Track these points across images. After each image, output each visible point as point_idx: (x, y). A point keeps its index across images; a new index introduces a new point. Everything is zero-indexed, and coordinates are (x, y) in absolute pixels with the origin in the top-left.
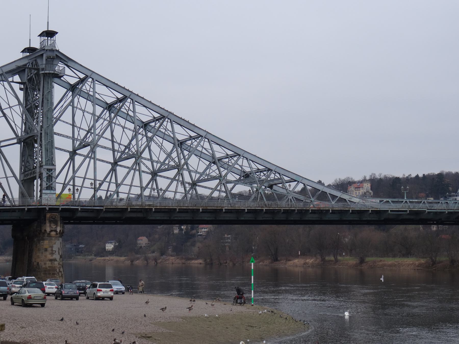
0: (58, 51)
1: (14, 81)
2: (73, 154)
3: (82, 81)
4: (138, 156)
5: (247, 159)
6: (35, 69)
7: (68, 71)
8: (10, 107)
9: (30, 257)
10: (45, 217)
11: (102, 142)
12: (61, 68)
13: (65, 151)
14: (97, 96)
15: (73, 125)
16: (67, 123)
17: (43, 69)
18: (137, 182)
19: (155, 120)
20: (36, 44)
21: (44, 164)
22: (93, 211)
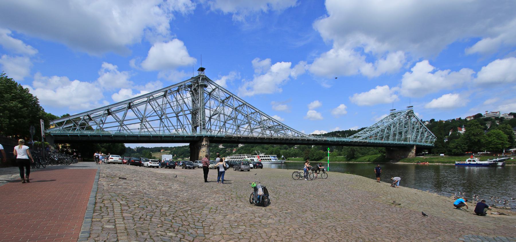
10: (203, 139)
19: (240, 106)
21: (202, 119)
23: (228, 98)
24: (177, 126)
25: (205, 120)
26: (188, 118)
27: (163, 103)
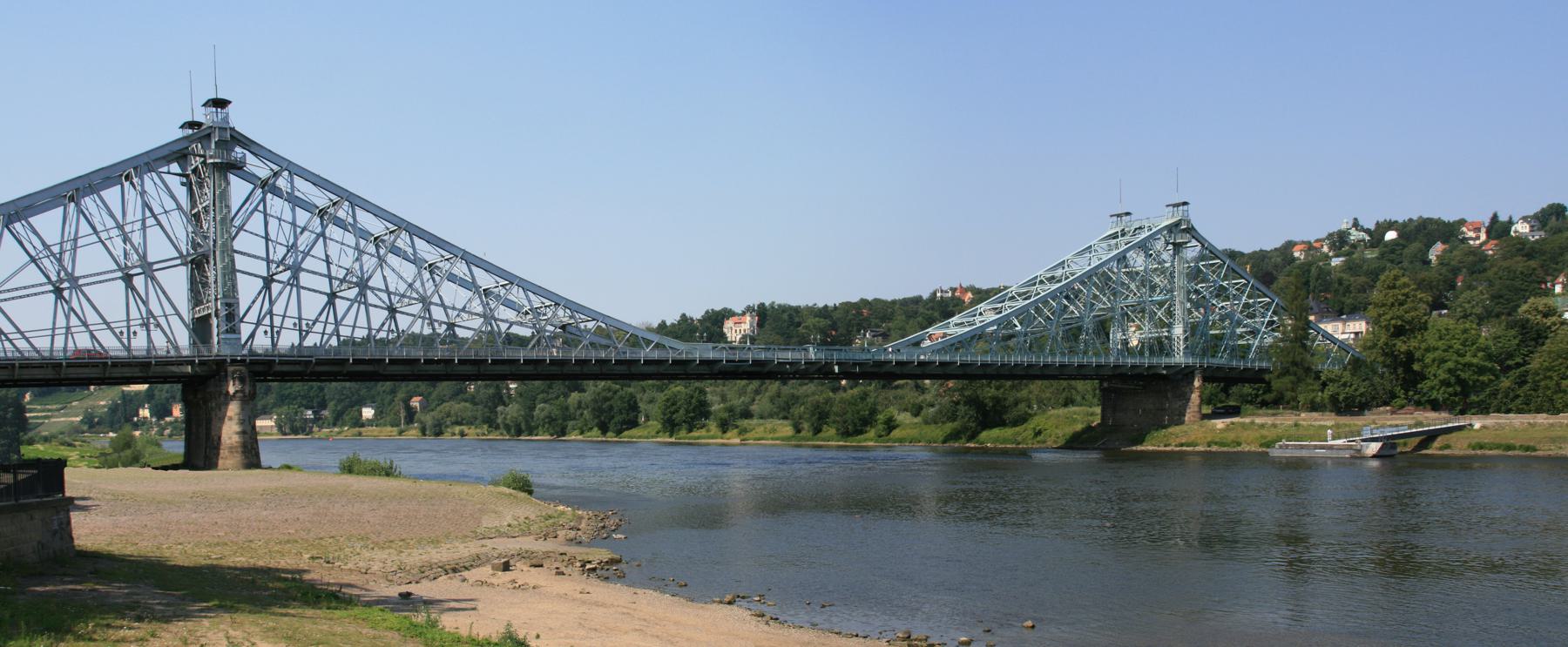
0: (233, 129)
1: (172, 171)
2: (268, 281)
3: (276, 175)
4: (363, 285)
5: (523, 289)
6: (200, 156)
7: (250, 159)
8: (166, 212)
9: (208, 430)
10: (226, 371)
11: (308, 263)
12: (239, 156)
13: (256, 276)
14: (297, 193)
15: (267, 238)
16: (257, 235)
17: (211, 157)
18: (362, 321)
20: (201, 115)
22: (299, 363)
23: (334, 204)
24: (128, 320)
25: (234, 297)
26: (164, 293)
27: (66, 239)
